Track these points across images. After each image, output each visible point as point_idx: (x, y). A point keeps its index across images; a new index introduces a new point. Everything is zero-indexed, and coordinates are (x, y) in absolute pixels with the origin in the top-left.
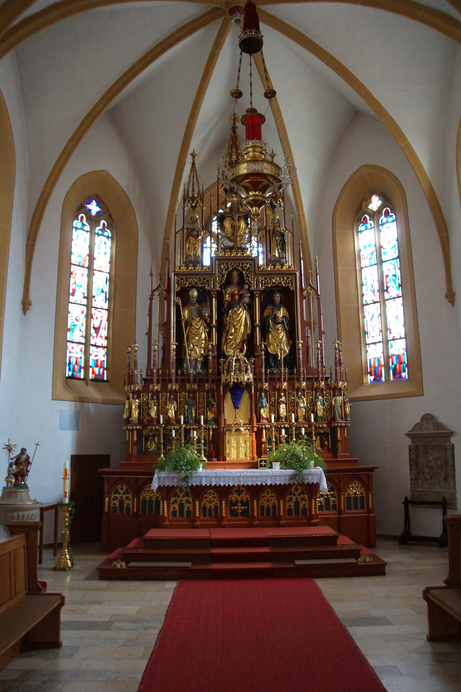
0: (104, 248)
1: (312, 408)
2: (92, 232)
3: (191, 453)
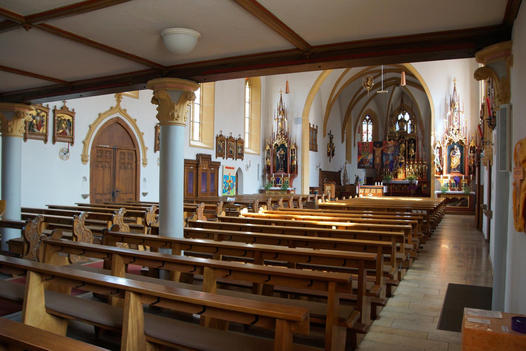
0: (370, 127)
1: (418, 168)
2: (368, 124)
3: (390, 177)
